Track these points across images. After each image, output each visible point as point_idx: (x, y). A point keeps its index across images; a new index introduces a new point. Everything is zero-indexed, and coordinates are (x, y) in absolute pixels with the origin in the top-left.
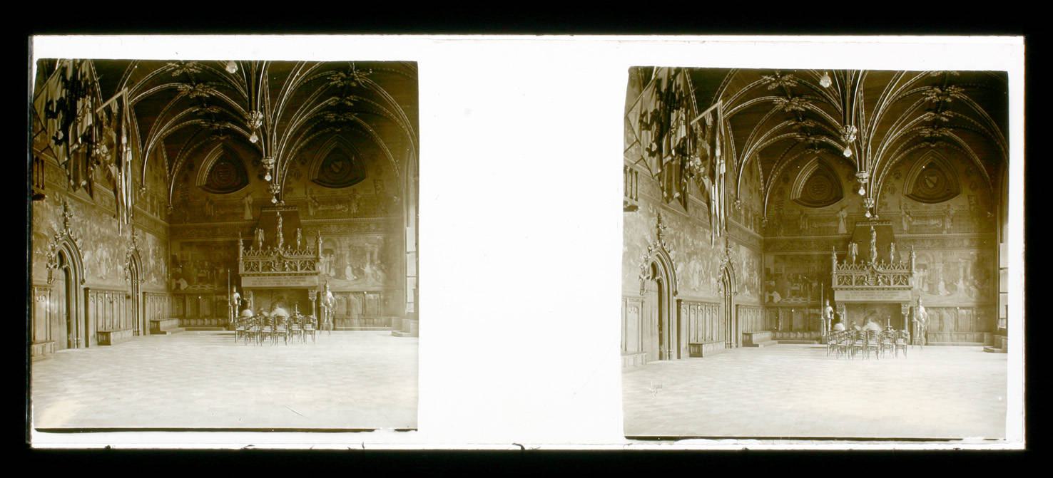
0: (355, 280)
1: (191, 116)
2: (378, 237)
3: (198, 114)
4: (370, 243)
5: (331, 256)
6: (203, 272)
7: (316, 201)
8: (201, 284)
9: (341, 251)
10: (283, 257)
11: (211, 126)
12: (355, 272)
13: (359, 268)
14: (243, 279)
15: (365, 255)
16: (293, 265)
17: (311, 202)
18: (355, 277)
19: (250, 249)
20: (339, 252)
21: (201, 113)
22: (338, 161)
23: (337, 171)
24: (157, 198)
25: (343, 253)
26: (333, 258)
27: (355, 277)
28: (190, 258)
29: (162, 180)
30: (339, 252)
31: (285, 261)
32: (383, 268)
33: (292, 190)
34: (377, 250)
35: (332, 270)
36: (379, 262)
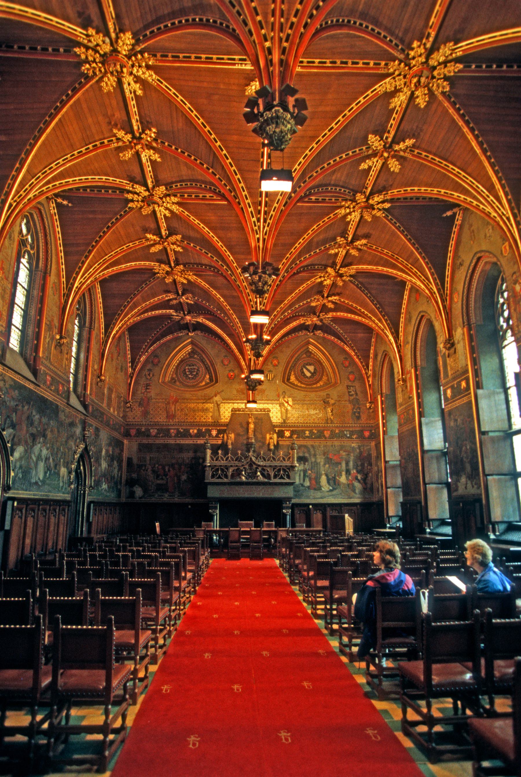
0: (331, 491)
1: (166, 305)
2: (353, 445)
3: (172, 303)
4: (345, 451)
5: (305, 464)
6: (162, 479)
7: (288, 404)
8: (159, 493)
9: (316, 458)
10: (254, 463)
11: (182, 318)
12: (331, 482)
13: (334, 478)
14: (209, 487)
15: (340, 464)
16: (266, 473)
17: (284, 405)
18: (331, 488)
19: (218, 454)
20: (313, 460)
21: (175, 302)
22: (310, 365)
23: (308, 374)
24: (116, 392)
25: (318, 461)
26: (307, 466)
27: (331, 488)
28: (148, 462)
29: (123, 373)
30: (313, 460)
31: (257, 468)
32: (359, 478)
33: (264, 391)
34: (352, 458)
35: (307, 479)
36: (355, 471)
